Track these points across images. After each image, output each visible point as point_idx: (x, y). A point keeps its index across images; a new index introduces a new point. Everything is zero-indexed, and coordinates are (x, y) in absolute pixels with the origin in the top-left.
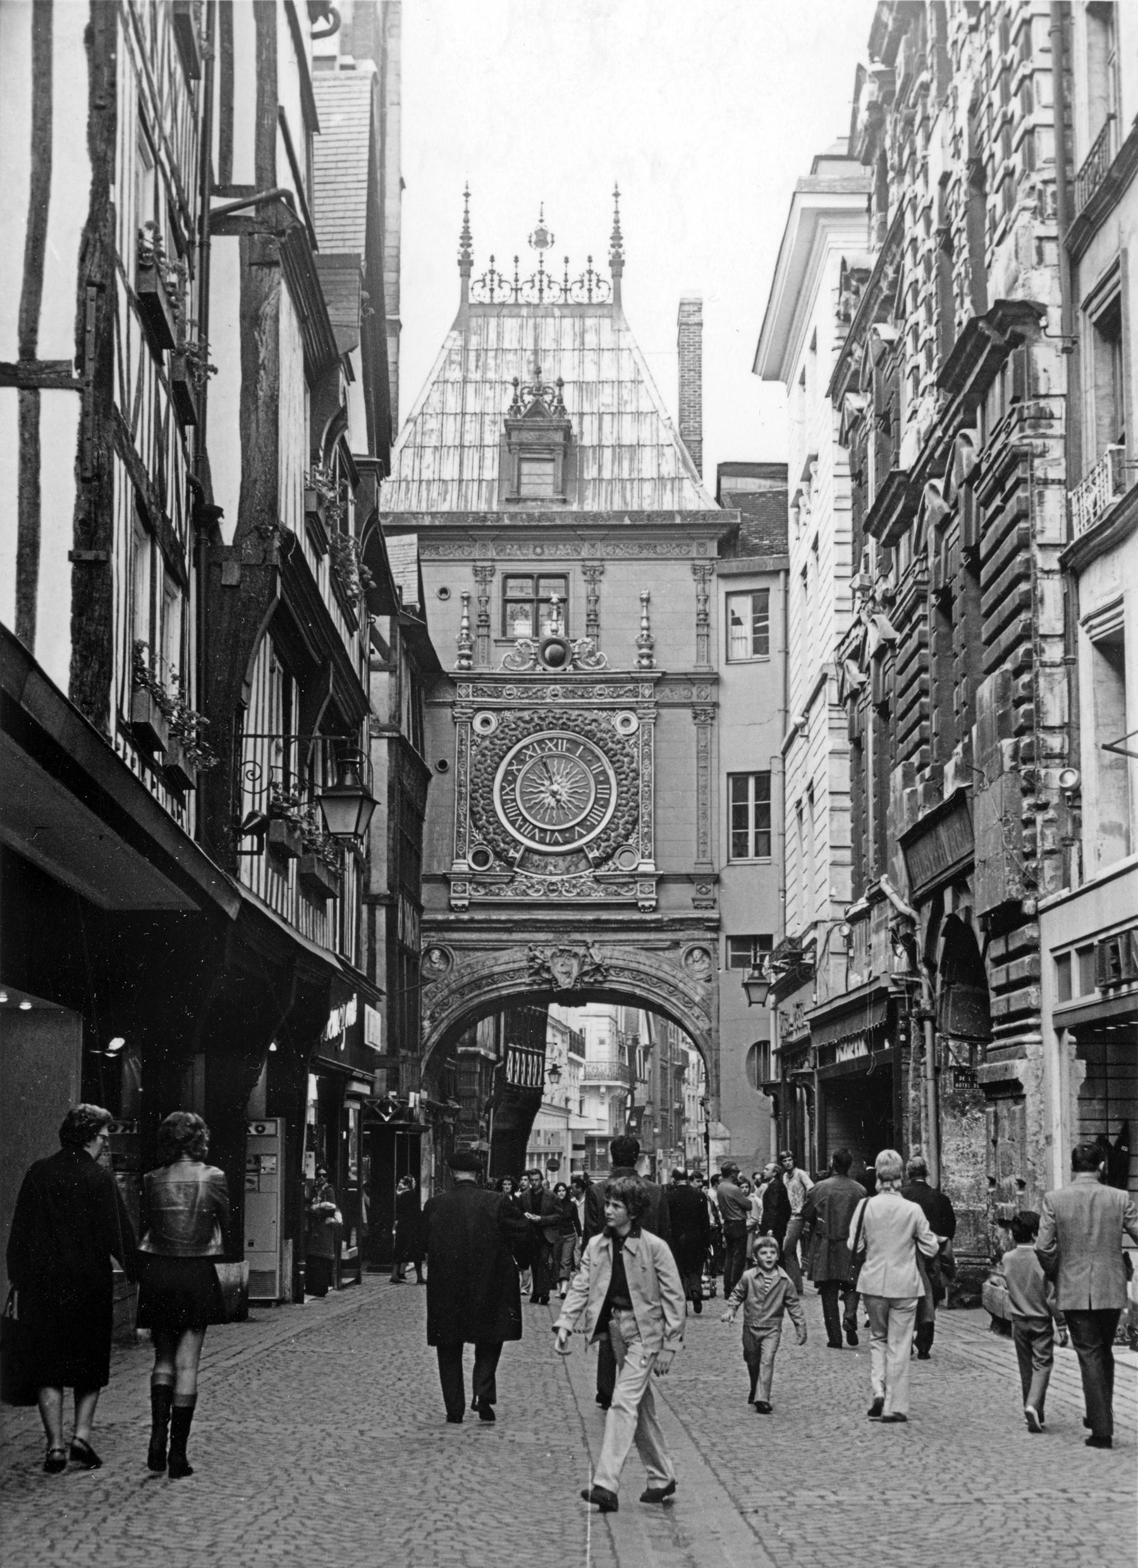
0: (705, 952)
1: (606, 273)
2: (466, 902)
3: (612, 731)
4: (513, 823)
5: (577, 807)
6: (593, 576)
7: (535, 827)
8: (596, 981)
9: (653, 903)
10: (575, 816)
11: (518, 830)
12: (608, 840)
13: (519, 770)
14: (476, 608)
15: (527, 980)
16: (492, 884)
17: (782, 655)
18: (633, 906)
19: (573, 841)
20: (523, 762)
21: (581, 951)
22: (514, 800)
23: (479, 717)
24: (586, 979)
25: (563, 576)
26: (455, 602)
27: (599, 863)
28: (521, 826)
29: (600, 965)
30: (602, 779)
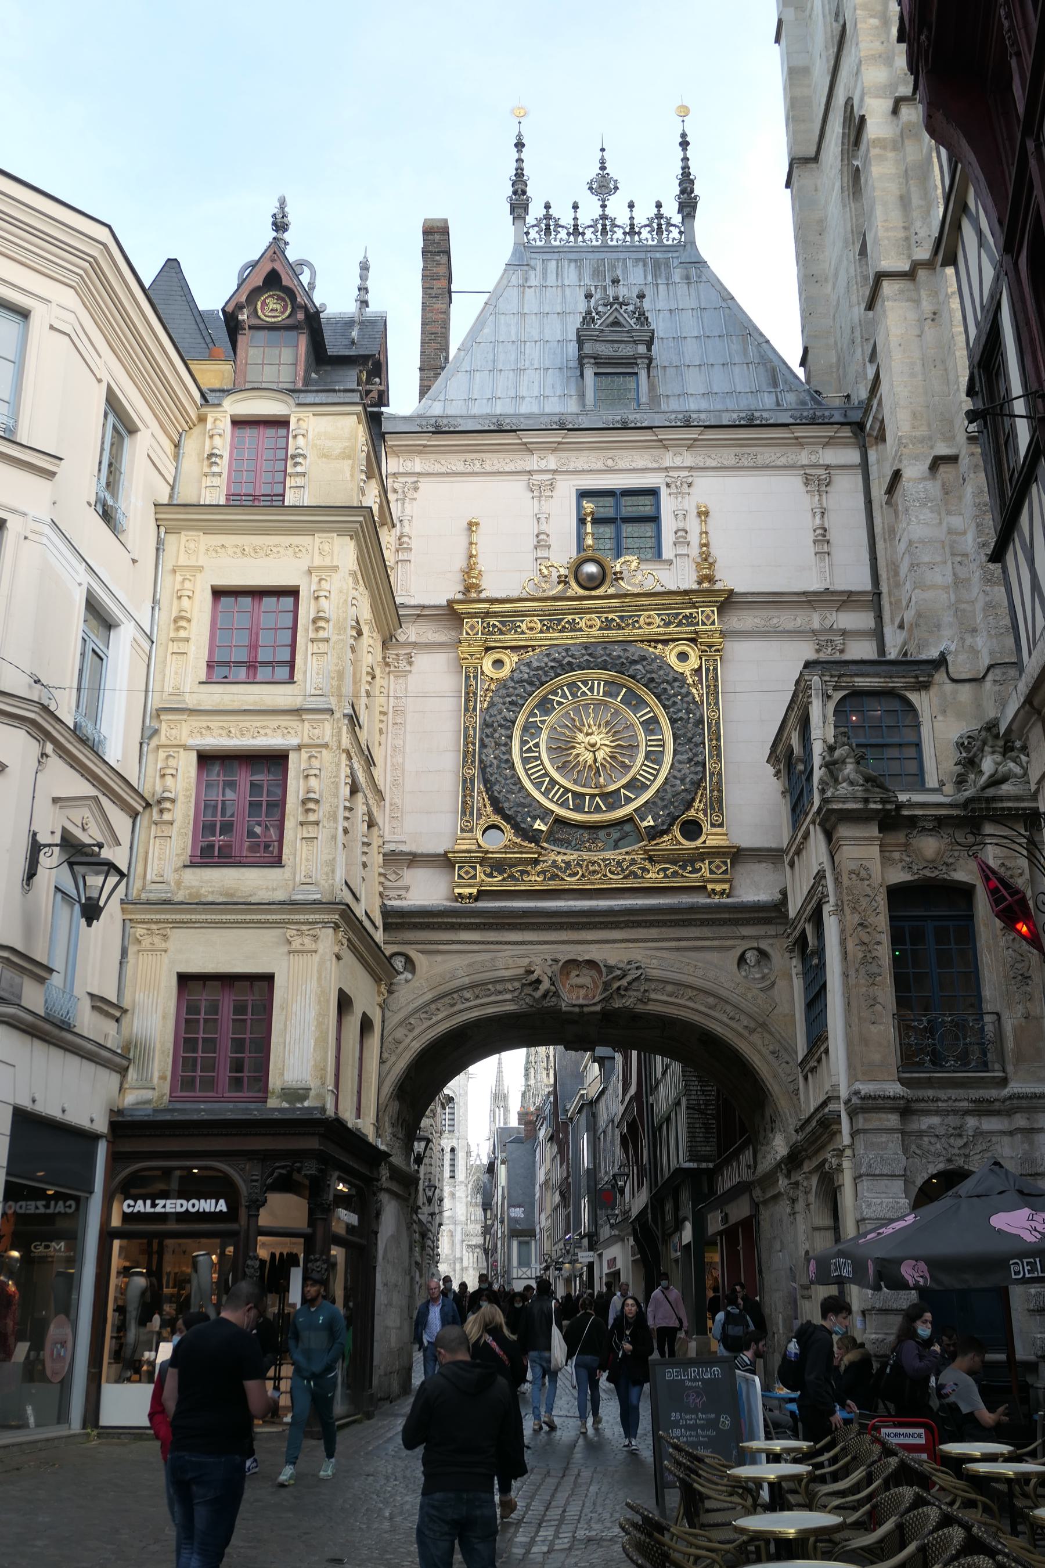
4: (538, 785)
7: (567, 790)
11: (546, 794)
22: (539, 758)
27: (654, 833)
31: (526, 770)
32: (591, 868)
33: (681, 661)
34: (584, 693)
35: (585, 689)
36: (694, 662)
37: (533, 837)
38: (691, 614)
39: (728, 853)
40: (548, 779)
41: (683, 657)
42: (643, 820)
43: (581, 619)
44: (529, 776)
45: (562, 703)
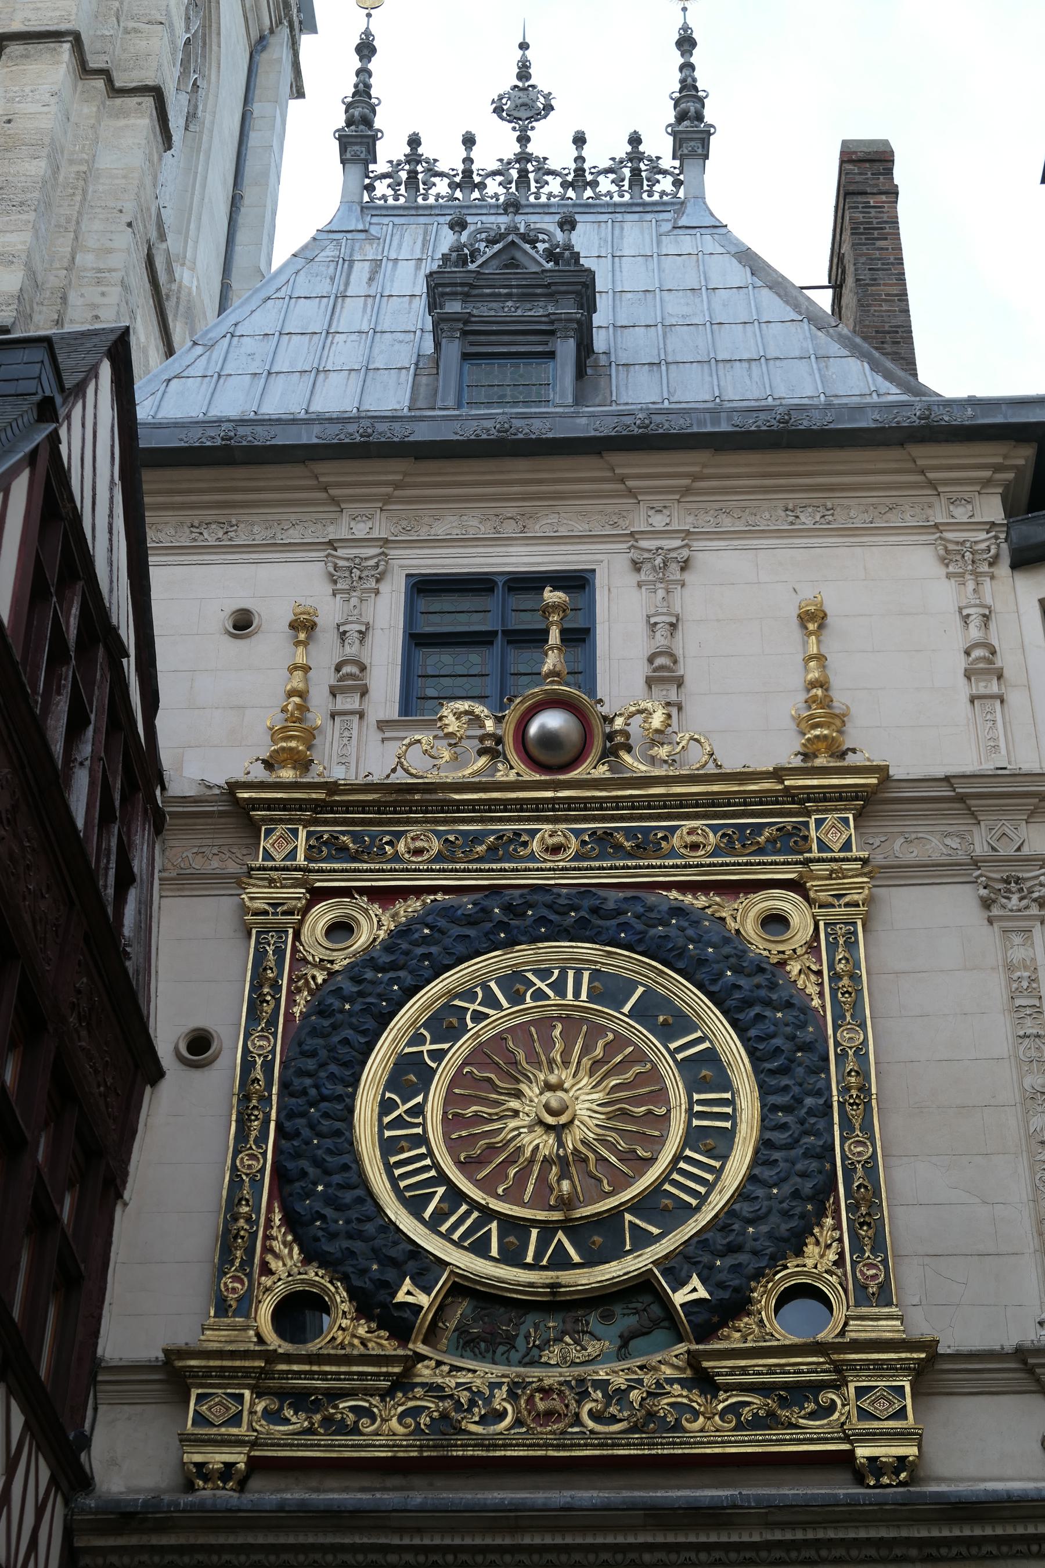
1: (668, 162)
2: (238, 1457)
4: (415, 1206)
5: (628, 1157)
7: (488, 1214)
9: (910, 1451)
10: (623, 1182)
11: (433, 1225)
12: (732, 1249)
13: (438, 1056)
14: (324, 655)
16: (335, 1395)
19: (619, 1254)
20: (454, 1033)
22: (422, 1140)
23: (322, 916)
25: (578, 582)
26: (272, 642)
28: (440, 1216)
30: (705, 1071)
31: (389, 1168)
32: (541, 1406)
33: (772, 923)
34: (539, 995)
35: (539, 984)
37: (399, 1323)
38: (796, 827)
39: (903, 1368)
40: (441, 1190)
42: (679, 1283)
43: (533, 833)
44: (394, 1181)
45: (487, 1016)
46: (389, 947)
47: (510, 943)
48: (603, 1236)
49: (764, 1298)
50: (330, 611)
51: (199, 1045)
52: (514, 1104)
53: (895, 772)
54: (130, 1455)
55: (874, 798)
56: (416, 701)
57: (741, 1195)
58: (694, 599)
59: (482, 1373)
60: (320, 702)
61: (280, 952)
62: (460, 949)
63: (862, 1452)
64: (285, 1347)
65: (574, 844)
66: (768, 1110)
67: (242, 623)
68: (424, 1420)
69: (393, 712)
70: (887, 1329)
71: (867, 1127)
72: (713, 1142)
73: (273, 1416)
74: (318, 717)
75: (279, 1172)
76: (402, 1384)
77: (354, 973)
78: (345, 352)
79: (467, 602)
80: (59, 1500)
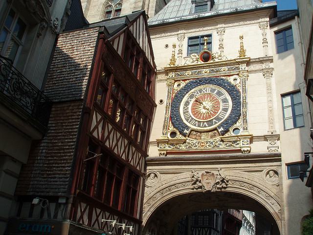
0: (276, 173)
3: (229, 84)
4: (187, 120)
6: (221, 33)
8: (223, 187)
9: (249, 149)
10: (213, 115)
12: (227, 124)
13: (190, 101)
15: (192, 187)
16: (176, 144)
17: (300, 44)
18: (239, 151)
19: (212, 125)
21: (216, 173)
22: (188, 112)
23: (176, 84)
24: (218, 186)
25: (210, 36)
28: (190, 121)
29: (224, 179)
34: (204, 92)
36: (238, 81)
41: (235, 79)
46: (185, 87)
47: (200, 85)
48: (210, 123)
49: (231, 130)
50: (177, 43)
51: (161, 101)
52: (200, 106)
53: (251, 58)
54: (153, 152)
55: (248, 63)
56: (189, 54)
57: (229, 117)
58: (224, 37)
59: (195, 141)
60: (176, 54)
61: (171, 89)
62: (194, 86)
63: (242, 149)
64: (172, 139)
65: (209, 71)
66: (233, 105)
67: (167, 46)
68: (187, 147)
69: (186, 56)
70: (247, 134)
71: (246, 107)
72: (226, 110)
73: (169, 147)
74: (176, 57)
75: (171, 117)
76: (185, 142)
77: (180, 91)
78: (182, 8)
79: (196, 40)
80: (143, 158)
